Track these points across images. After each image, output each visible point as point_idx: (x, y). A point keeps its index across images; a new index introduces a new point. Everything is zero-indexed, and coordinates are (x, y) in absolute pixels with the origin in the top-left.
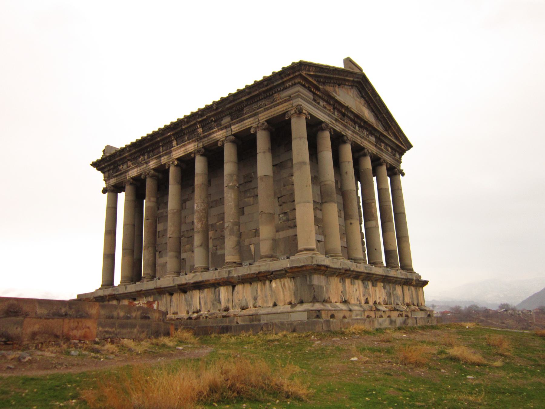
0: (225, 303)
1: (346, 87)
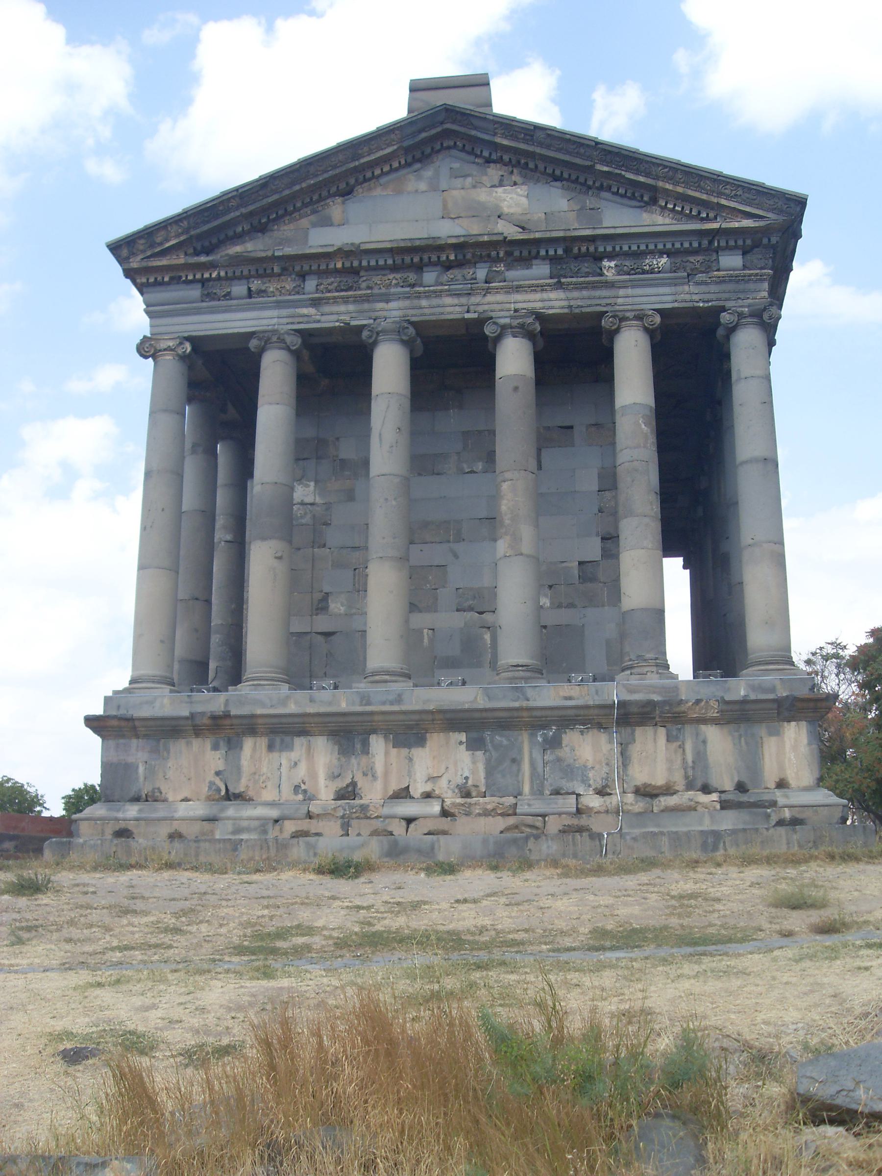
1: (383, 180)
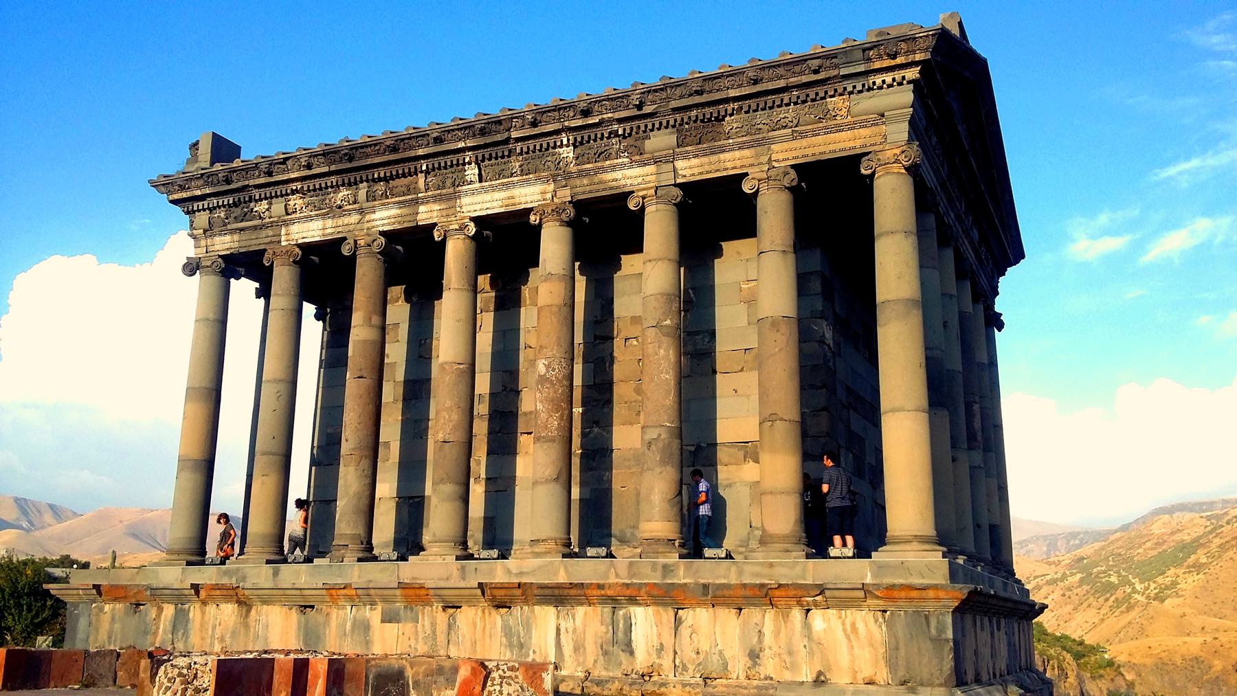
0: (650, 655)
